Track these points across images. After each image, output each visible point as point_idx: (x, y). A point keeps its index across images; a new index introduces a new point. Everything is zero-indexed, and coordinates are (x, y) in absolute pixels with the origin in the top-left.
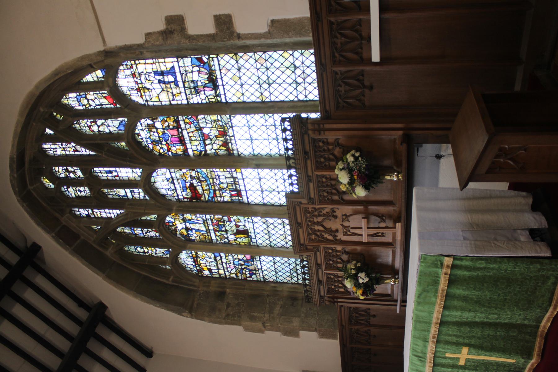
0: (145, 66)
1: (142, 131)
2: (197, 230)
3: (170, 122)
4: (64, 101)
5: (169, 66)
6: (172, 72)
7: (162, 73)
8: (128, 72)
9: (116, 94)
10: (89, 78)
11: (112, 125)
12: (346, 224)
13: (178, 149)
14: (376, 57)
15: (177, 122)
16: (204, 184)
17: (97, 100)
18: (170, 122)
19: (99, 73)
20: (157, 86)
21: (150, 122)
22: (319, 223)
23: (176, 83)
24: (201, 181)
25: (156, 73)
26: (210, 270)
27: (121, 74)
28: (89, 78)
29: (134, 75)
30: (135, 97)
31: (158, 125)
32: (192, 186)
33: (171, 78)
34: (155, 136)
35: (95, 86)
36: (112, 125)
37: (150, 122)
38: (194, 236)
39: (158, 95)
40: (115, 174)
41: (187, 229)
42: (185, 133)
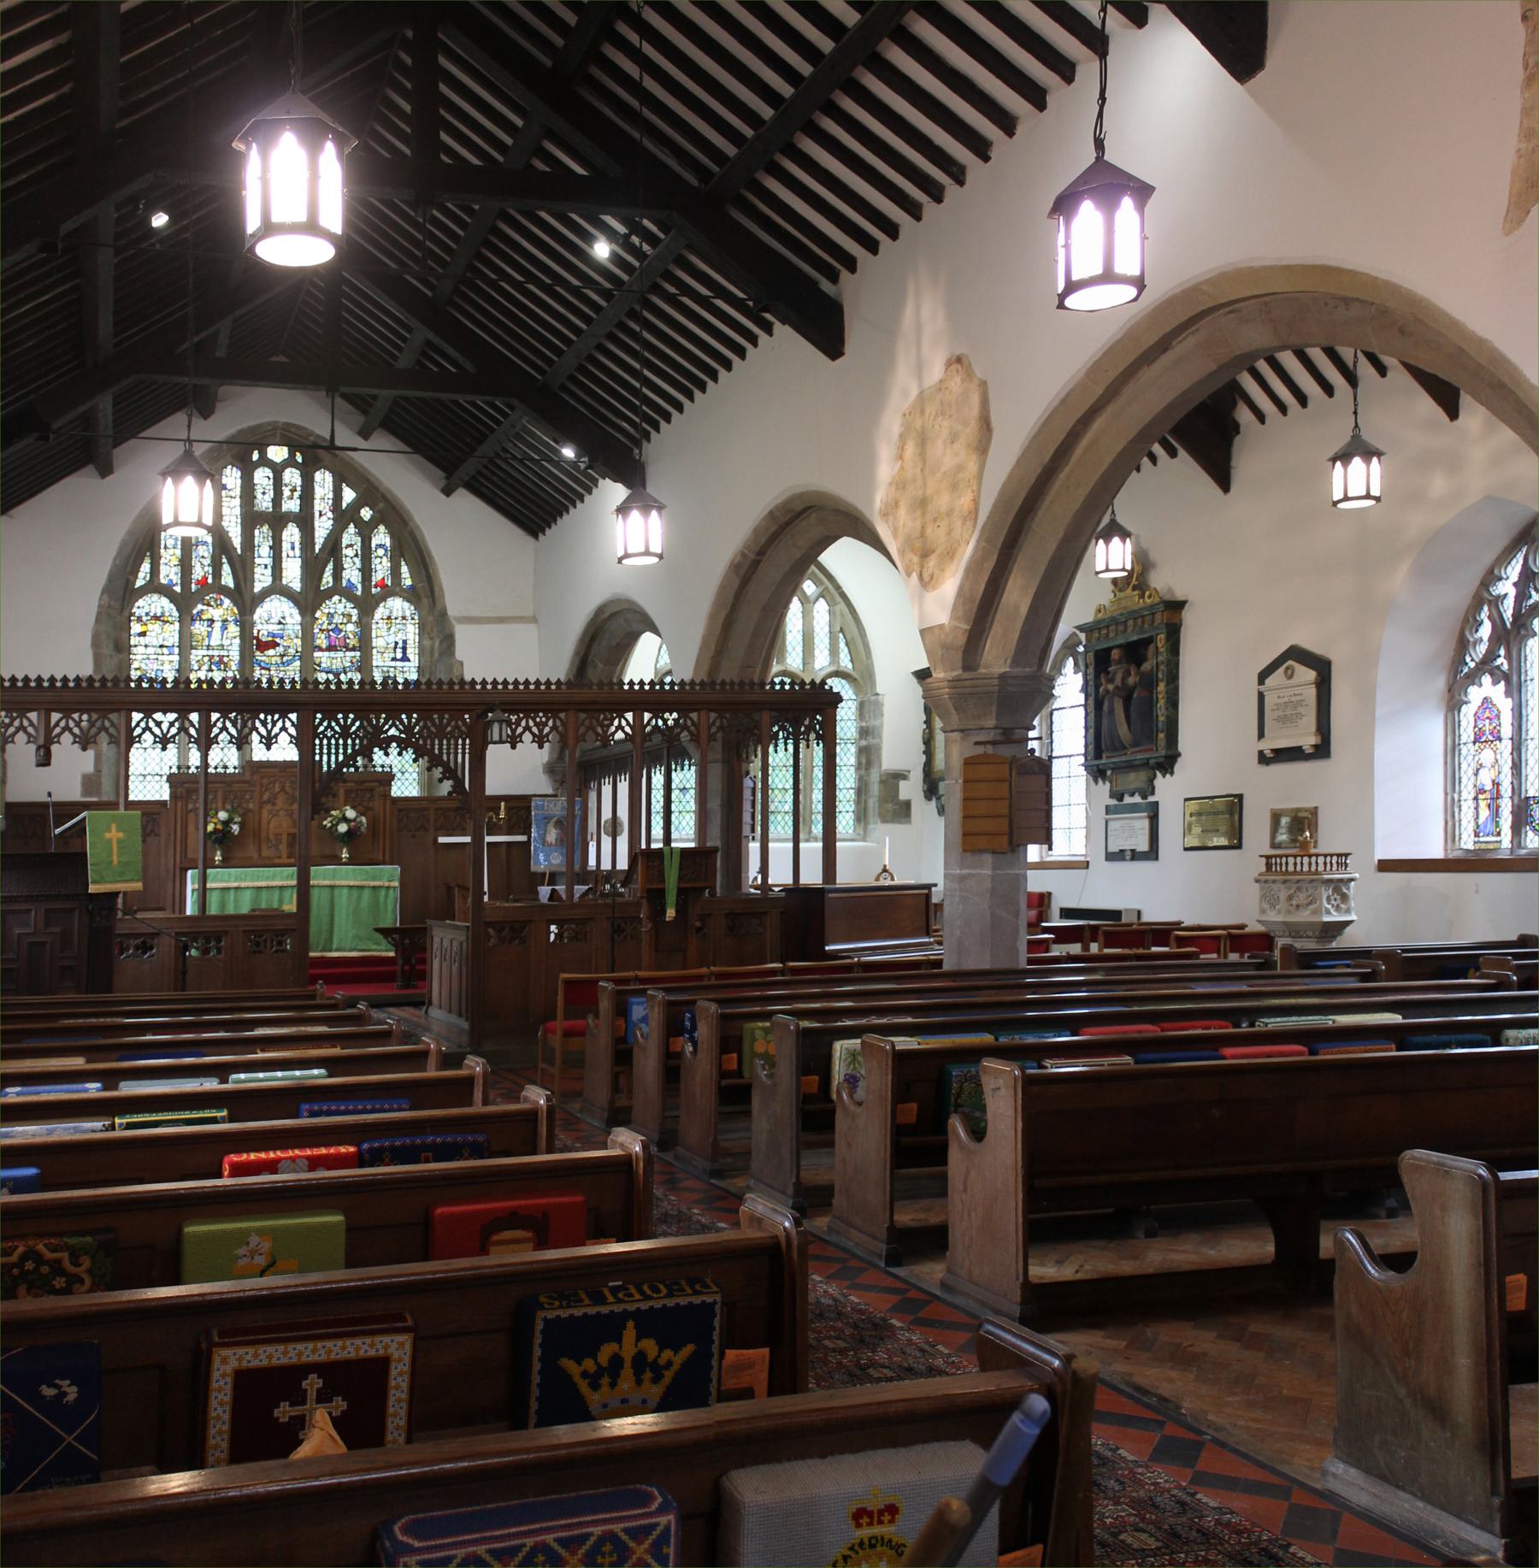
0: (411, 633)
1: (338, 606)
2: (209, 635)
3: (352, 642)
4: (382, 528)
5: (411, 656)
6: (405, 658)
7: (404, 649)
8: (408, 613)
9: (387, 592)
10: (404, 569)
11: (352, 574)
12: (282, 813)
13: (322, 641)
14: (442, 840)
15: (353, 649)
16: (278, 660)
17: (381, 568)
18: (352, 642)
19: (408, 582)
20: (391, 639)
21: (354, 618)
22: (283, 789)
23: (394, 659)
24: (282, 656)
25: (405, 642)
26: (143, 634)
27: (406, 605)
28: (404, 569)
29: (404, 618)
30: (380, 612)
31: (350, 627)
32: (274, 645)
33: (399, 656)
34: (337, 619)
35: (395, 572)
36: (352, 574)
37: (354, 618)
38: (199, 628)
39: (382, 638)
40: (291, 553)
41: (212, 621)
42: (341, 654)
